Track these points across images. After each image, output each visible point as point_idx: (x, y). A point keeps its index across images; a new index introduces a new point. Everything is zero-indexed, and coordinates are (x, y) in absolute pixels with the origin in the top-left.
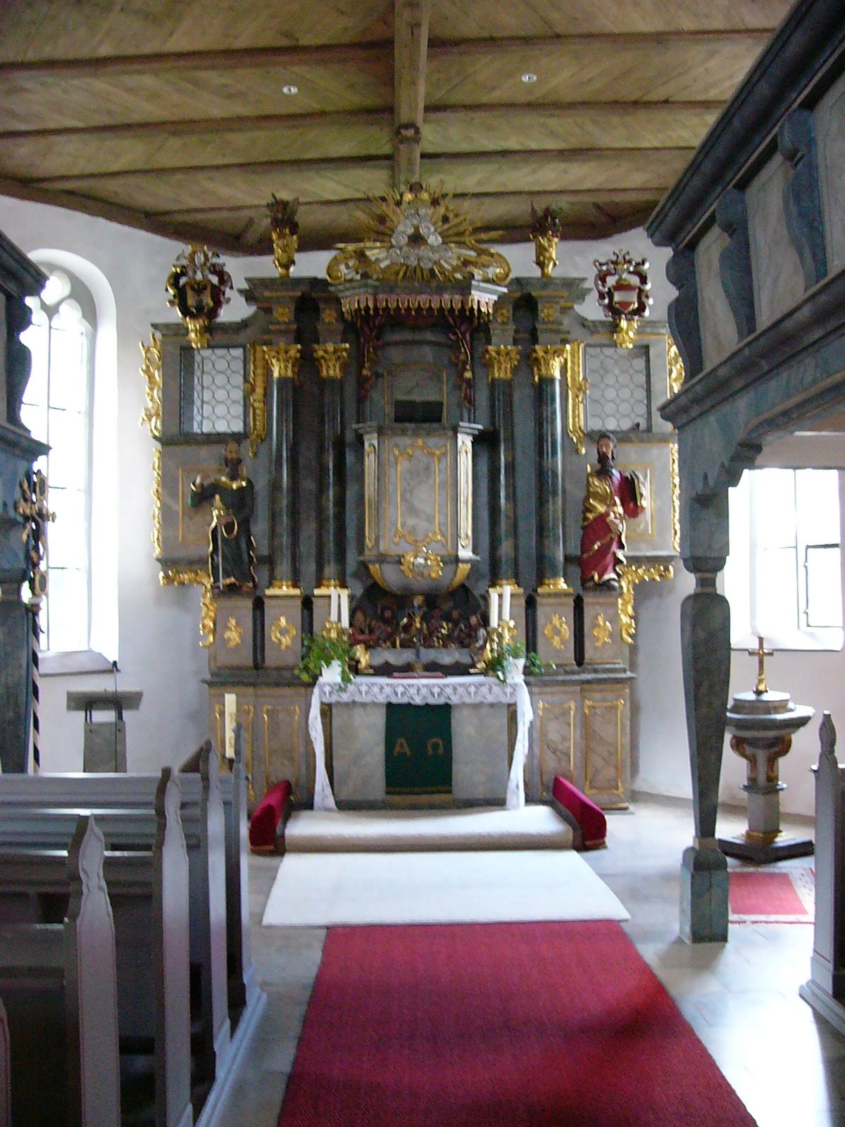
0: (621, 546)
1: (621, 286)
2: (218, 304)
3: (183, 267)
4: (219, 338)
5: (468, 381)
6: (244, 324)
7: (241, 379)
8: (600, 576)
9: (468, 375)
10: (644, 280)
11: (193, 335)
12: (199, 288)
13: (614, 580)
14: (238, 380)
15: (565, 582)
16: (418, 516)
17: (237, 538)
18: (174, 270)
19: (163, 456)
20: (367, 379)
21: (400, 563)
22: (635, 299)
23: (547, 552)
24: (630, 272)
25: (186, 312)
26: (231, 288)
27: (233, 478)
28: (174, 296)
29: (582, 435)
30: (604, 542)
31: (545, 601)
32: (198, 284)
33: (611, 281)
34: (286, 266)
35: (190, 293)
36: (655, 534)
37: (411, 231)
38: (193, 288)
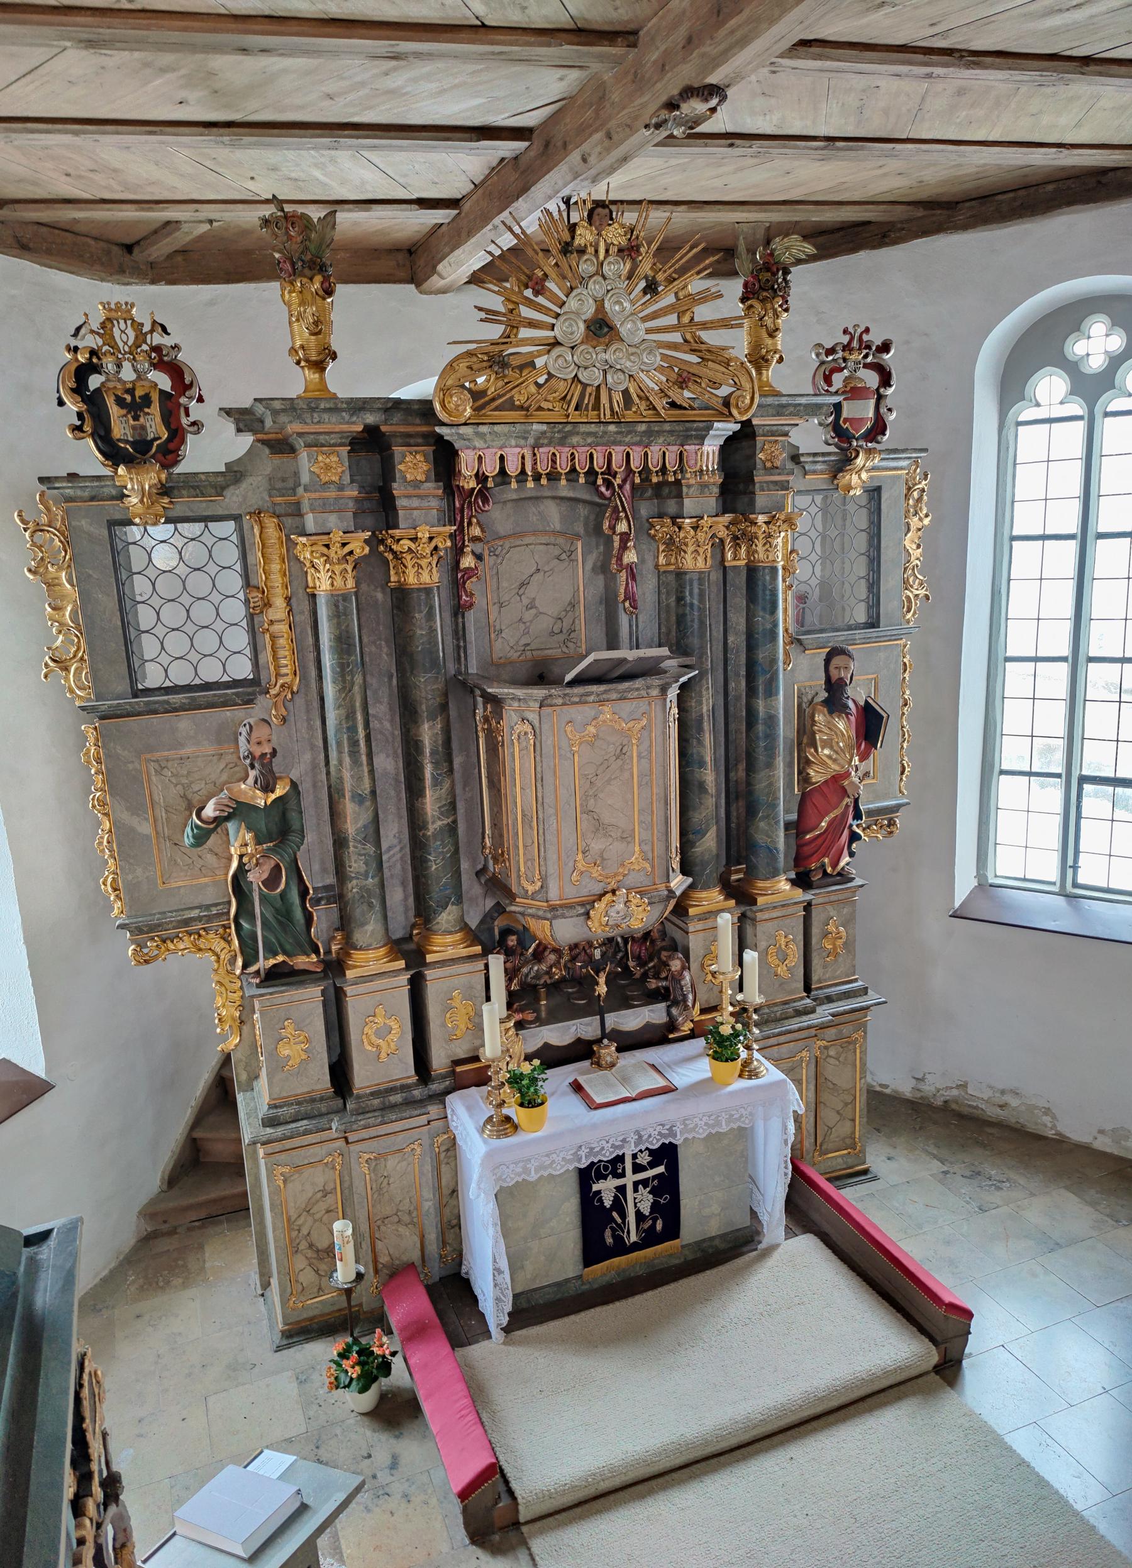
0: (858, 815)
1: (854, 392)
2: (177, 435)
3: (93, 353)
4: (183, 504)
5: (630, 568)
6: (235, 473)
7: (239, 582)
8: (835, 865)
9: (631, 557)
10: (886, 379)
11: (134, 500)
12: (136, 406)
14: (233, 582)
16: (607, 835)
17: (283, 895)
18: (69, 356)
19: (102, 737)
20: (470, 572)
21: (587, 915)
22: (871, 414)
23: (761, 839)
24: (866, 366)
25: (113, 453)
26: (200, 400)
27: (267, 788)
28: (80, 416)
31: (766, 915)
32: (131, 391)
33: (838, 380)
34: (319, 366)
35: (114, 411)
37: (589, 310)
38: (120, 402)
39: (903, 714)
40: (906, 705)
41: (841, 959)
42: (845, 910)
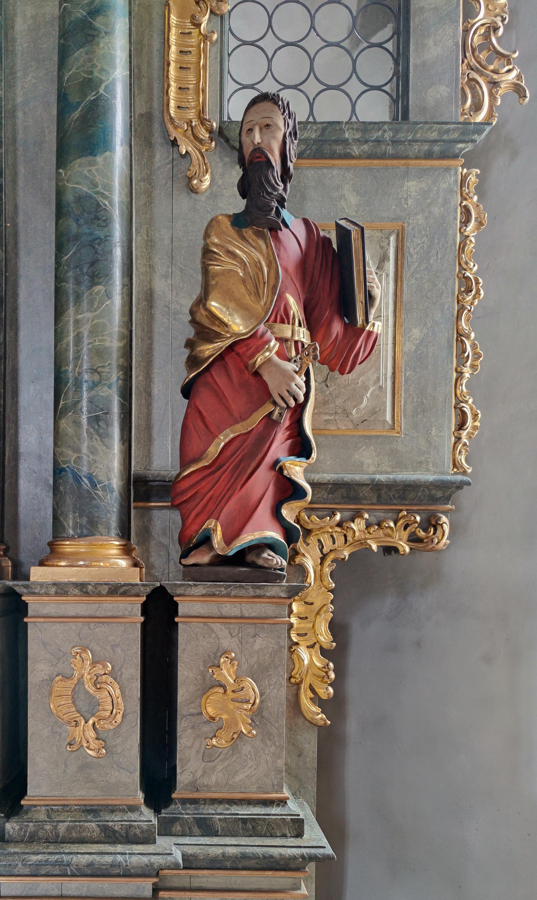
13: (272, 546)
15: (127, 551)
29: (204, 135)
30: (240, 429)
36: (403, 423)
39: (462, 308)
40: (469, 290)
41: (246, 749)
42: (259, 643)
